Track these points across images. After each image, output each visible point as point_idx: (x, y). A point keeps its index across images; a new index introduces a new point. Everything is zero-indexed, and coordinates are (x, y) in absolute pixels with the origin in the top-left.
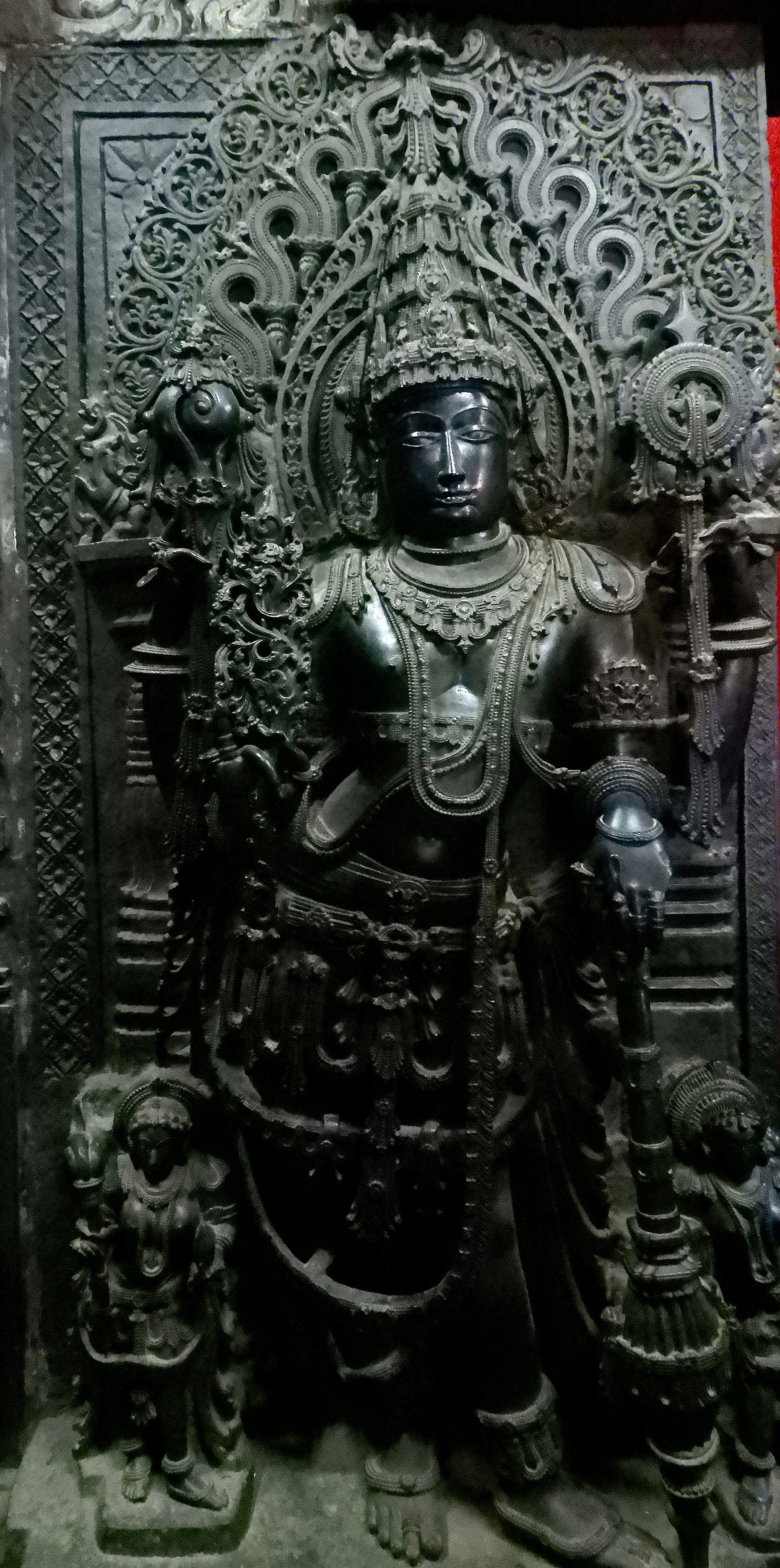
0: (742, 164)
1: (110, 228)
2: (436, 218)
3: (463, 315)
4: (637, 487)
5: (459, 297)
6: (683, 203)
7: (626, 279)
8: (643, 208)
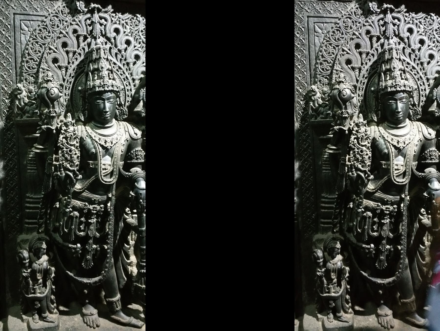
7: (433, 62)
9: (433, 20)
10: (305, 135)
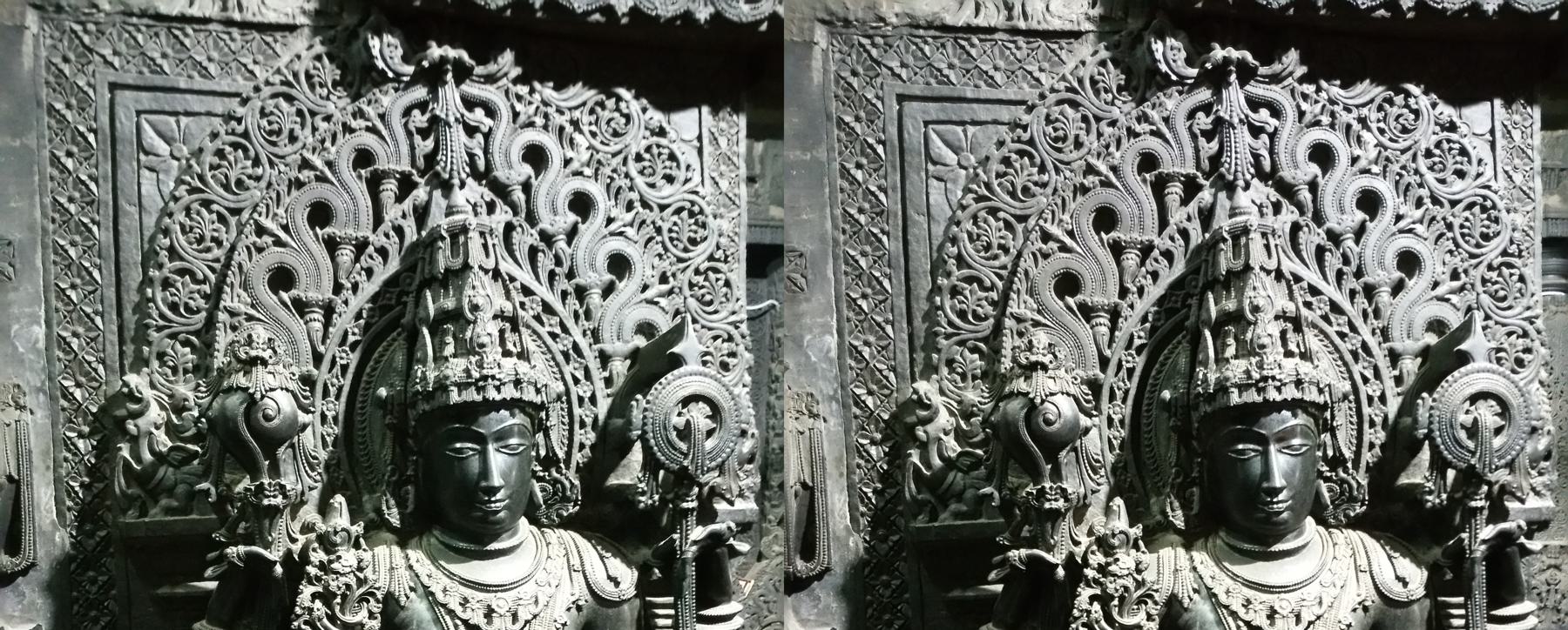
9: (1417, 113)
10: (887, 585)
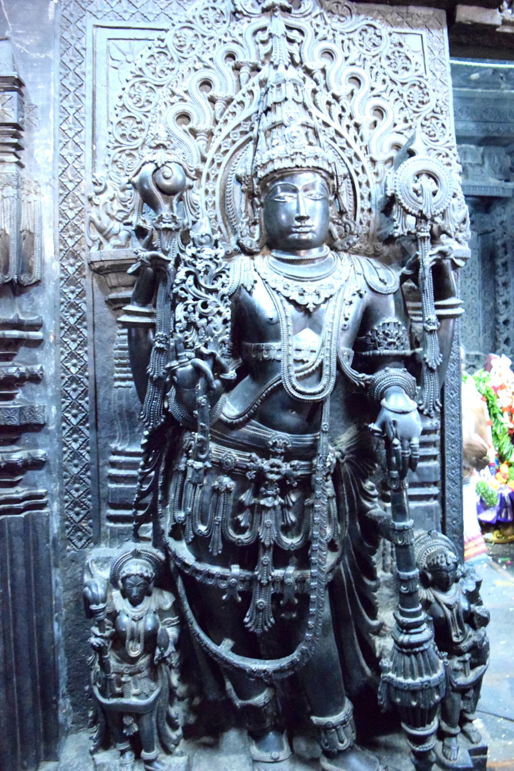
0: (438, 74)
1: (111, 84)
2: (291, 85)
3: (307, 134)
4: (397, 228)
5: (305, 125)
6: (411, 90)
7: (384, 124)
8: (392, 91)
